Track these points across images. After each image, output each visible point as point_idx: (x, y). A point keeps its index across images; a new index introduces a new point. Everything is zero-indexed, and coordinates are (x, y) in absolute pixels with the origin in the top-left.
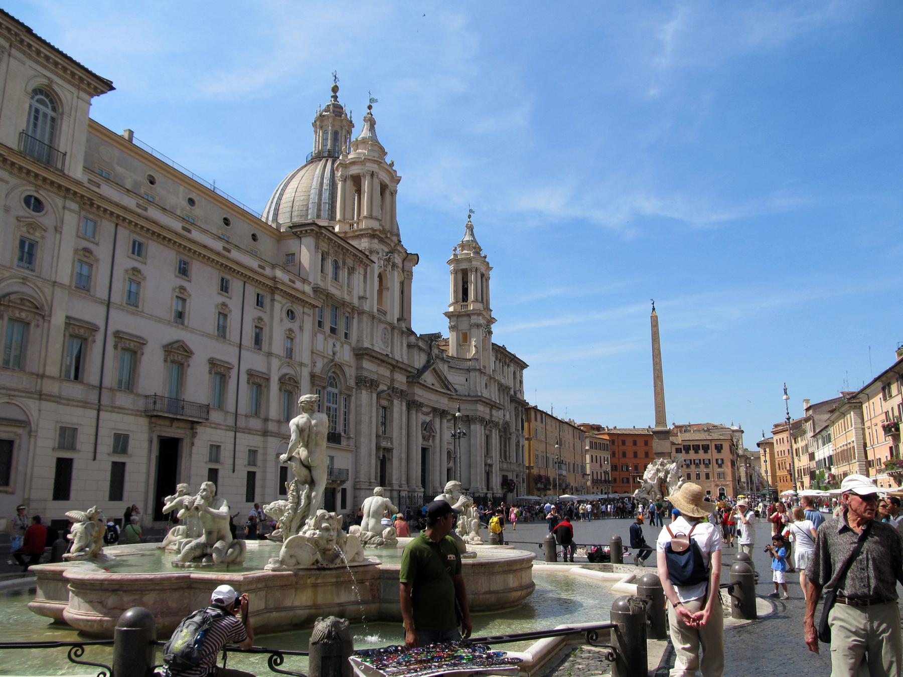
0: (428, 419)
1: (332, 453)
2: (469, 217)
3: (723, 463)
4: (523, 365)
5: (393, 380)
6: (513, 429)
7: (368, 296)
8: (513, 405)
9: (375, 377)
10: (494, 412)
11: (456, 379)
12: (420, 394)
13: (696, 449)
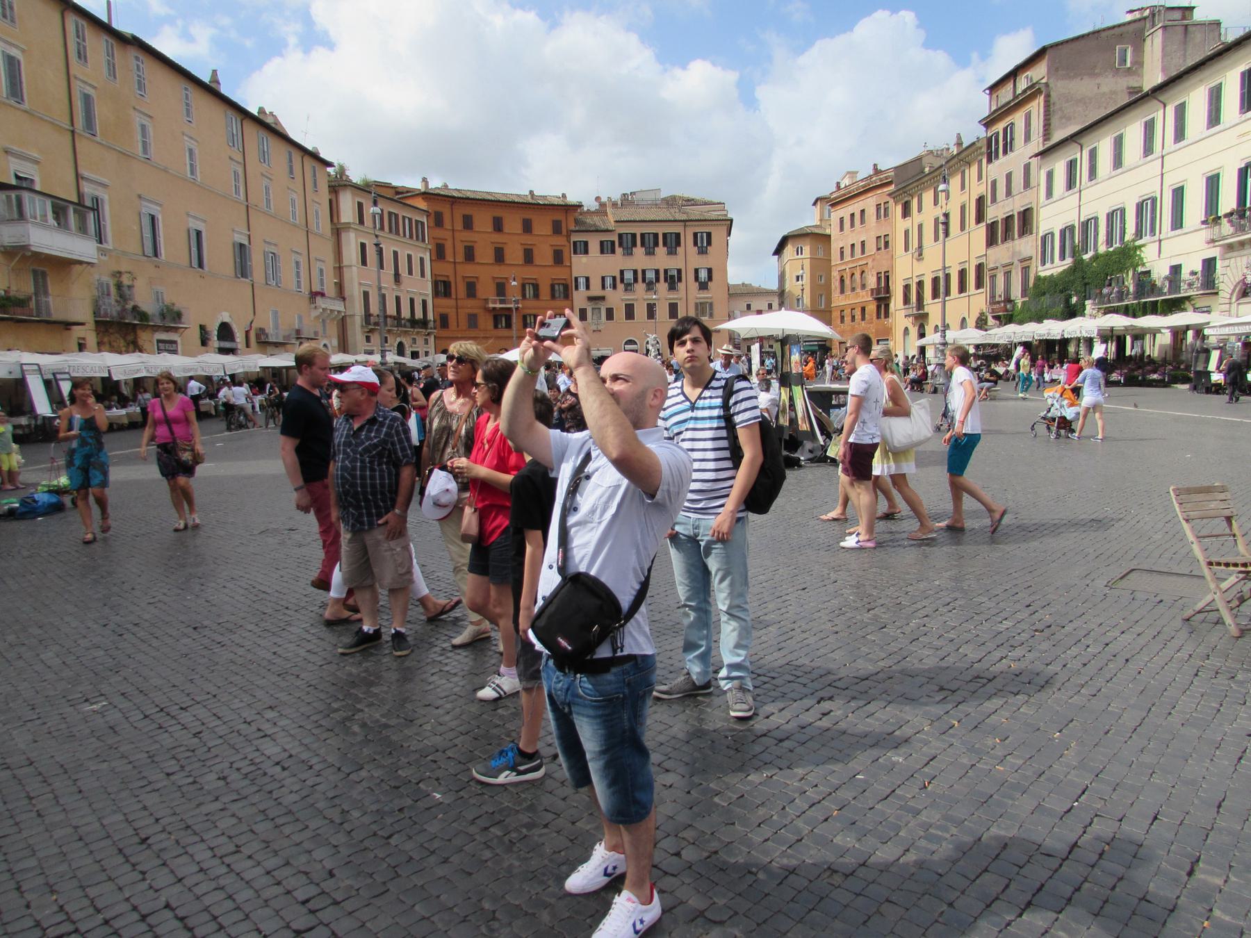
3: (710, 278)
13: (650, 243)
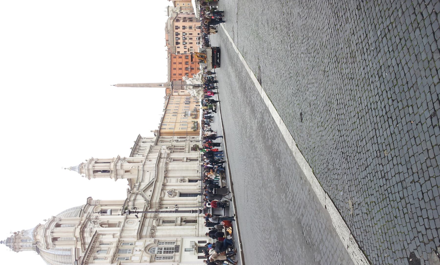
0: (167, 194)
1: (183, 250)
2: (65, 169)
4: (139, 138)
5: (151, 218)
6: (169, 144)
7: (113, 233)
8: (159, 143)
9: (150, 228)
10: (163, 156)
11: (148, 178)
12: (156, 200)
